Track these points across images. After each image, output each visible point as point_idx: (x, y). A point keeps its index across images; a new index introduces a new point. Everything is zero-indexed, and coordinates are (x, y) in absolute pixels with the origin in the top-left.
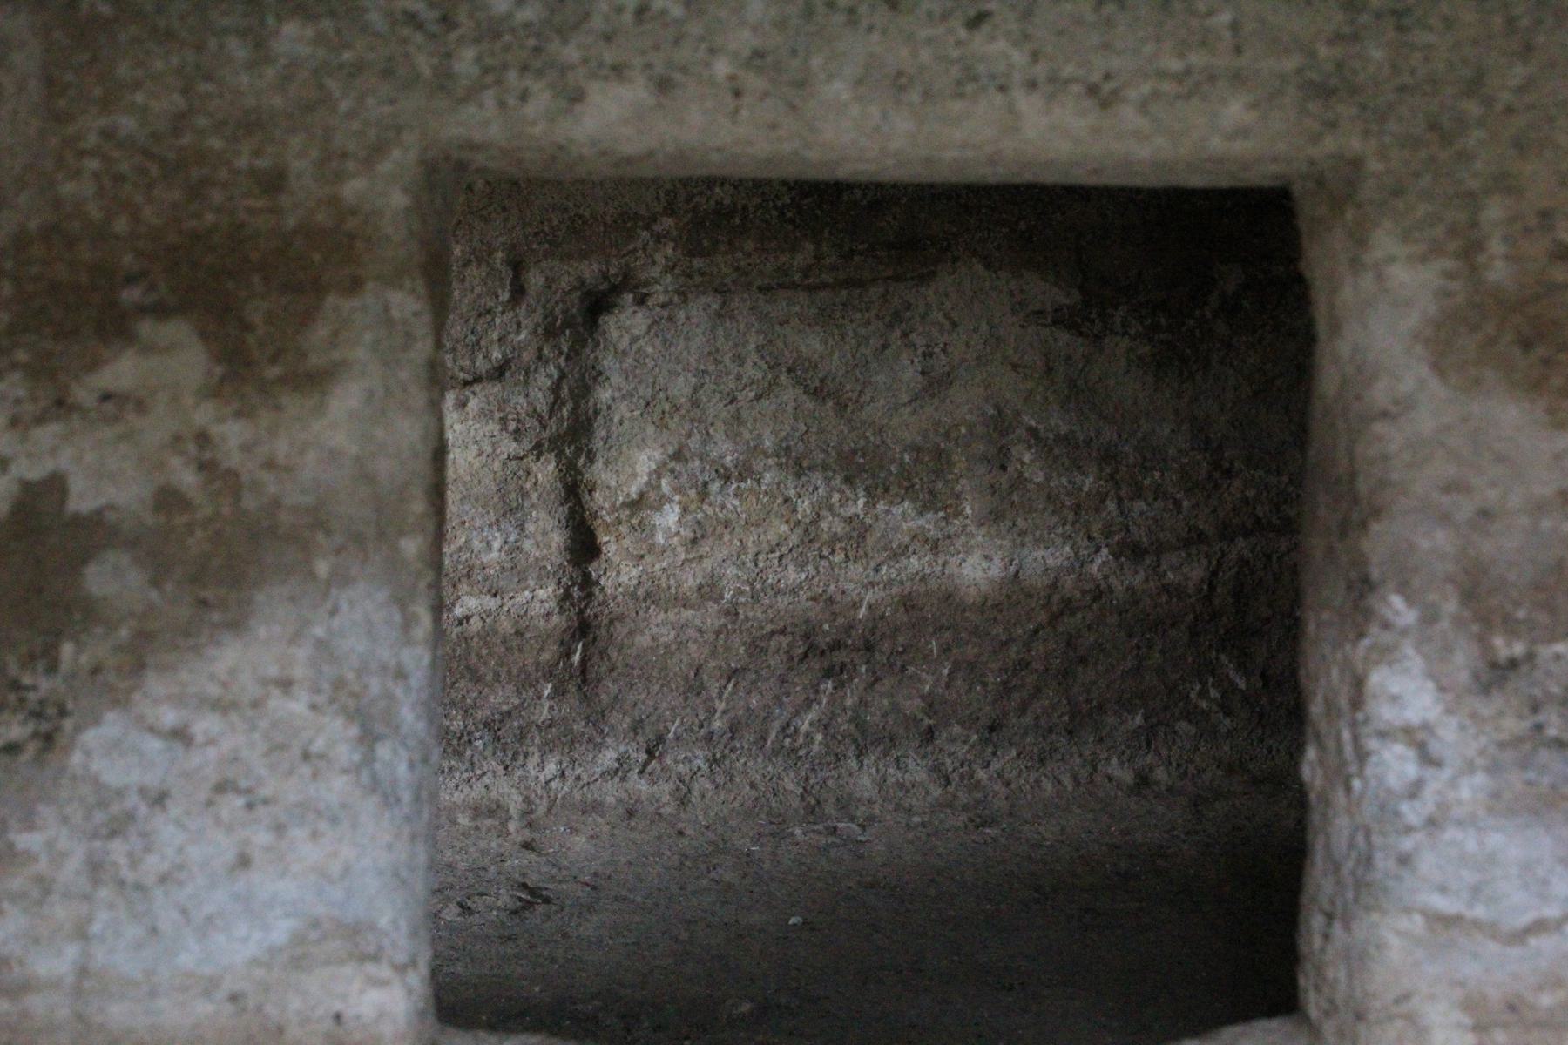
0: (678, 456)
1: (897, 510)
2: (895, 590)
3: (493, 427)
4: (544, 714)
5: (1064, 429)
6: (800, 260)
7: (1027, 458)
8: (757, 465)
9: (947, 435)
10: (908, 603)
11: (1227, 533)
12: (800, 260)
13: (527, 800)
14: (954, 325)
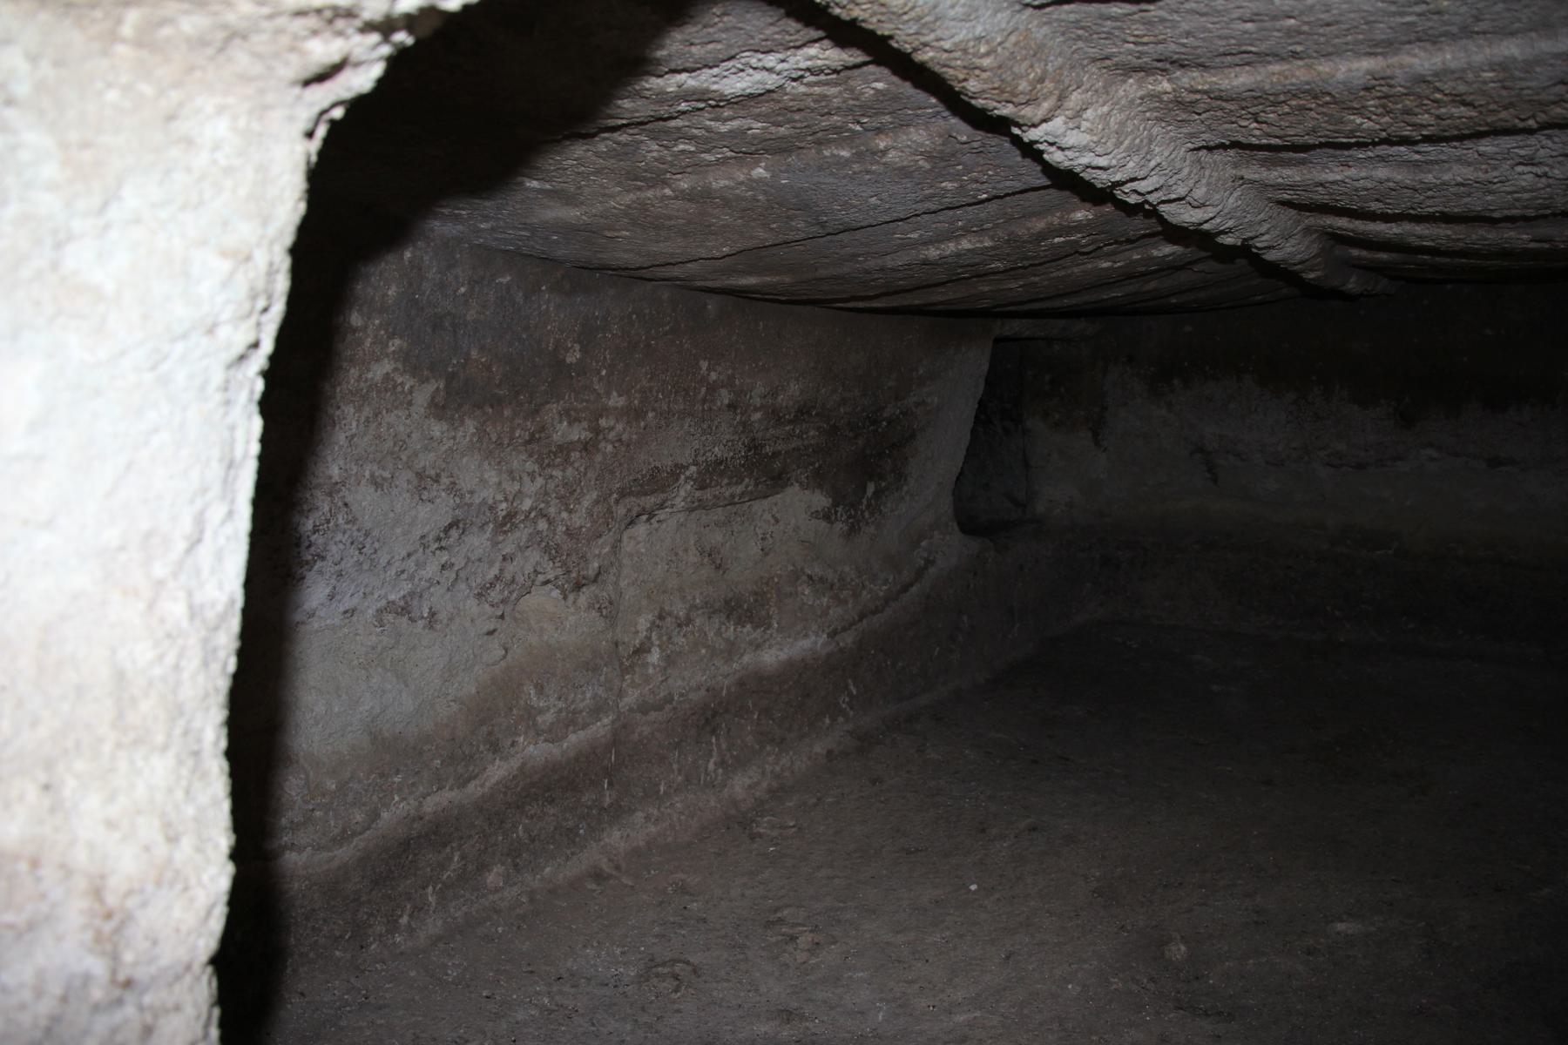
0: (661, 617)
3: (594, 614)
4: (607, 801)
6: (739, 489)
10: (741, 683)
12: (739, 489)
13: (610, 860)
14: (777, 521)
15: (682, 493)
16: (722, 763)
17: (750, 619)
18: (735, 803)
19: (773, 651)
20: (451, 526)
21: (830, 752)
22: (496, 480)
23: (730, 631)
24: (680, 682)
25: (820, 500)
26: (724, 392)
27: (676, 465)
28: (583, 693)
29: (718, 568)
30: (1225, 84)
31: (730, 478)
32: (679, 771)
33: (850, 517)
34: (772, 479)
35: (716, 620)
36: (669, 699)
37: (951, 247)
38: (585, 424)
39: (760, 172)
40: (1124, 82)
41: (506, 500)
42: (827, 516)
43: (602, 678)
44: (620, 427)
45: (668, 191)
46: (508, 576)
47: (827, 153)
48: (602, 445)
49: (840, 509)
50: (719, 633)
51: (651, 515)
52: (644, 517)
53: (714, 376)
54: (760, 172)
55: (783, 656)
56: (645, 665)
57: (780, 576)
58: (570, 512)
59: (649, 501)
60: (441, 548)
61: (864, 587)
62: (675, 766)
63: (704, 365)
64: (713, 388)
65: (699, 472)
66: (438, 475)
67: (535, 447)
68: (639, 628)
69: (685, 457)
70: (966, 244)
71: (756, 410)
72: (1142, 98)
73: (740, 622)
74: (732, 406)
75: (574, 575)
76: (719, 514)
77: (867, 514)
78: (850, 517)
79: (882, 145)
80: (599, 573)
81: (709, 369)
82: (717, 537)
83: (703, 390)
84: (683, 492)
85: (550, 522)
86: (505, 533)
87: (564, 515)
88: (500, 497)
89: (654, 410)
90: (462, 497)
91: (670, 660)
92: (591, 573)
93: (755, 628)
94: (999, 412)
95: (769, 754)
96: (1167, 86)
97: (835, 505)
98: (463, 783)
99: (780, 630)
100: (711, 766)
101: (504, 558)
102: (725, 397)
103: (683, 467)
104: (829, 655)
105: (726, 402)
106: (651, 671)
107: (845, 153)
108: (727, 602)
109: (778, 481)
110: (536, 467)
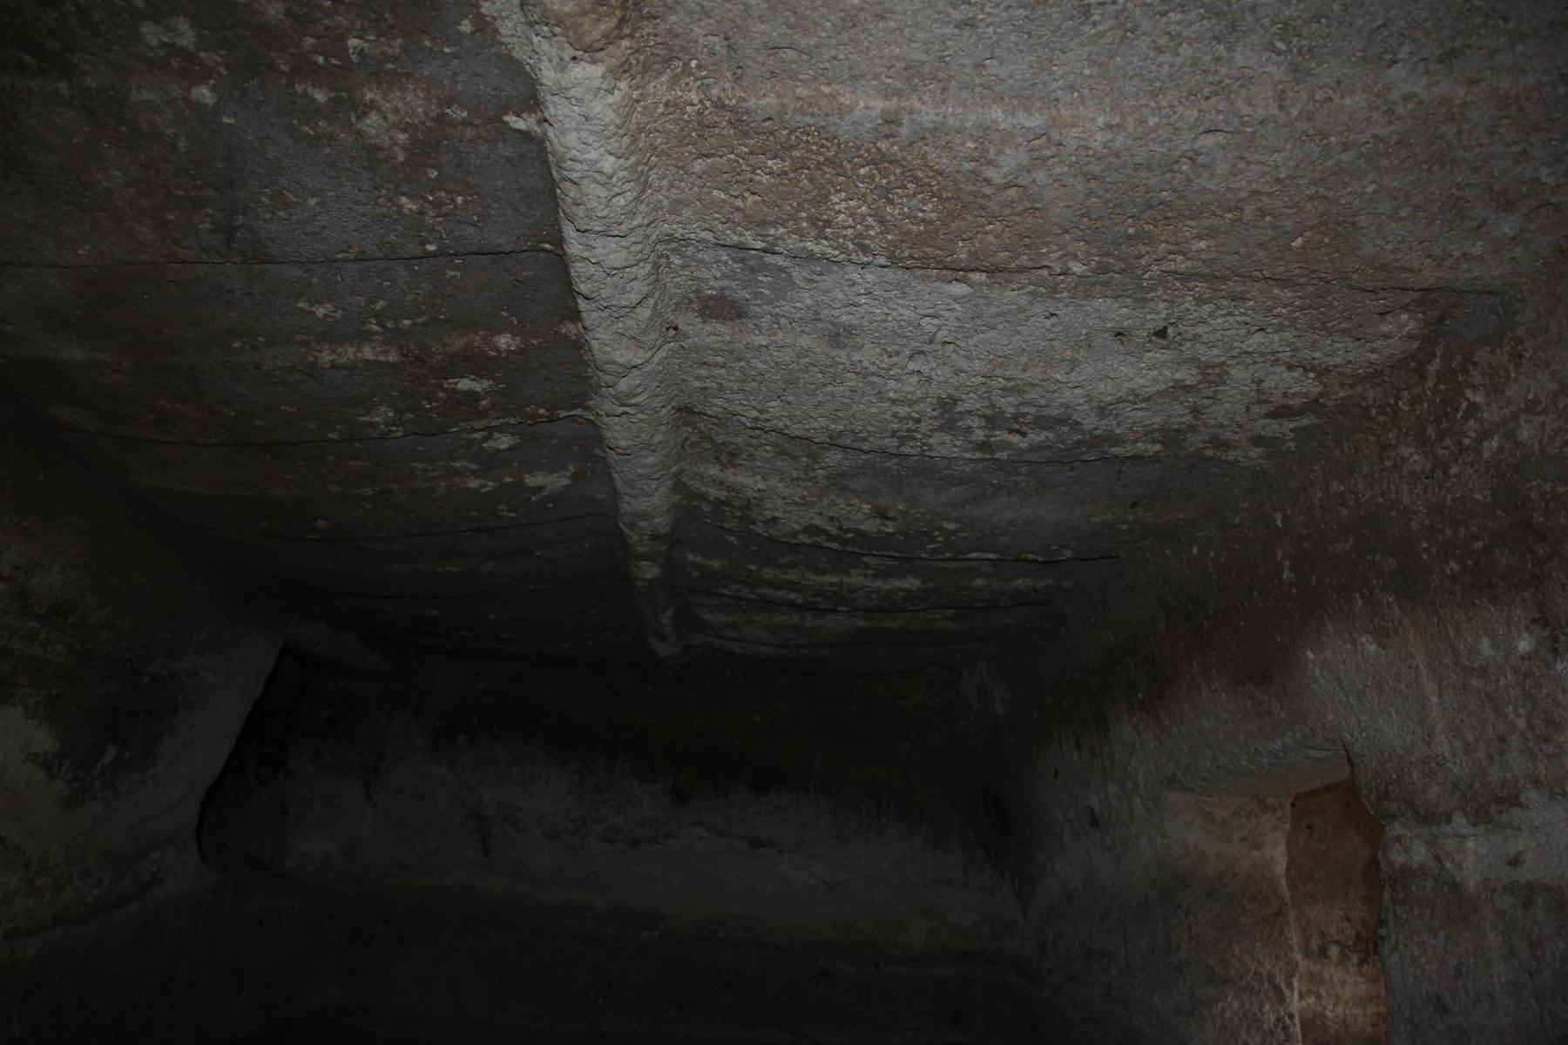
25: (45, 740)
30: (751, 103)
37: (348, 353)
39: (204, 94)
40: (660, 74)
47: (299, 88)
49: (67, 763)
54: (204, 94)
70: (368, 353)
72: (667, 105)
77: (97, 785)
79: (369, 96)
94: (262, 746)
96: (694, 97)
107: (320, 96)
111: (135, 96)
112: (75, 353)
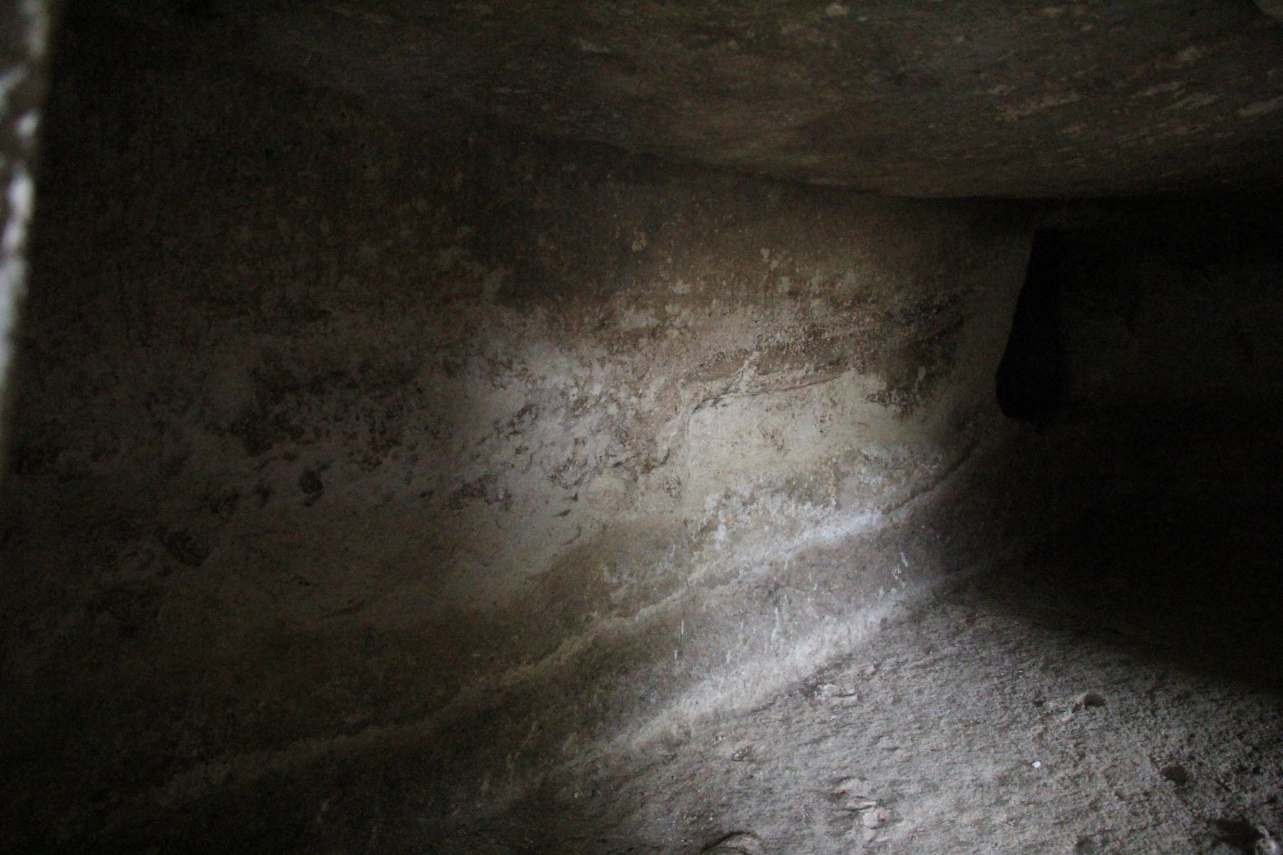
0: (727, 497)
1: (806, 507)
2: (798, 551)
5: (876, 454)
7: (864, 470)
8: (757, 494)
9: (826, 463)
10: (802, 558)
11: (913, 497)
12: (801, 373)
14: (835, 404)
15: (746, 377)
16: (785, 633)
17: (810, 497)
18: (796, 670)
19: (832, 527)
20: (524, 411)
21: (884, 620)
22: (566, 366)
23: (792, 509)
24: (745, 558)
25: (874, 383)
26: (785, 280)
27: (740, 351)
28: (654, 569)
29: (780, 449)
31: (792, 363)
32: (745, 641)
33: (903, 400)
34: (831, 363)
35: (779, 499)
36: (735, 573)
37: (1031, 107)
38: (652, 311)
41: (577, 384)
42: (882, 399)
43: (672, 555)
44: (685, 313)
45: (732, 43)
46: (580, 459)
48: (669, 332)
49: (894, 392)
50: (781, 510)
51: (717, 400)
52: (710, 402)
53: (775, 264)
55: (842, 532)
56: (712, 542)
57: (838, 457)
58: (640, 396)
59: (716, 386)
60: (515, 433)
61: (916, 466)
62: (740, 636)
63: (765, 253)
64: (774, 276)
65: (762, 357)
66: (510, 362)
67: (603, 332)
68: (707, 507)
69: (748, 343)
70: (1049, 101)
71: (815, 296)
73: (801, 500)
74: (793, 294)
75: (643, 458)
76: (779, 398)
78: (903, 400)
80: (667, 457)
81: (770, 257)
82: (775, 421)
83: (765, 277)
84: (747, 374)
85: (620, 406)
86: (577, 417)
87: (634, 399)
88: (571, 382)
89: (718, 297)
90: (534, 382)
91: (736, 537)
92: (661, 455)
93: (815, 505)
95: (827, 624)
97: (890, 388)
98: (536, 660)
99: (838, 507)
100: (774, 635)
101: (576, 441)
102: (785, 284)
103: (746, 352)
104: (884, 530)
105: (787, 289)
106: (718, 547)
108: (788, 482)
109: (837, 365)
110: (606, 353)
111: (785, 31)
112: (811, 160)
